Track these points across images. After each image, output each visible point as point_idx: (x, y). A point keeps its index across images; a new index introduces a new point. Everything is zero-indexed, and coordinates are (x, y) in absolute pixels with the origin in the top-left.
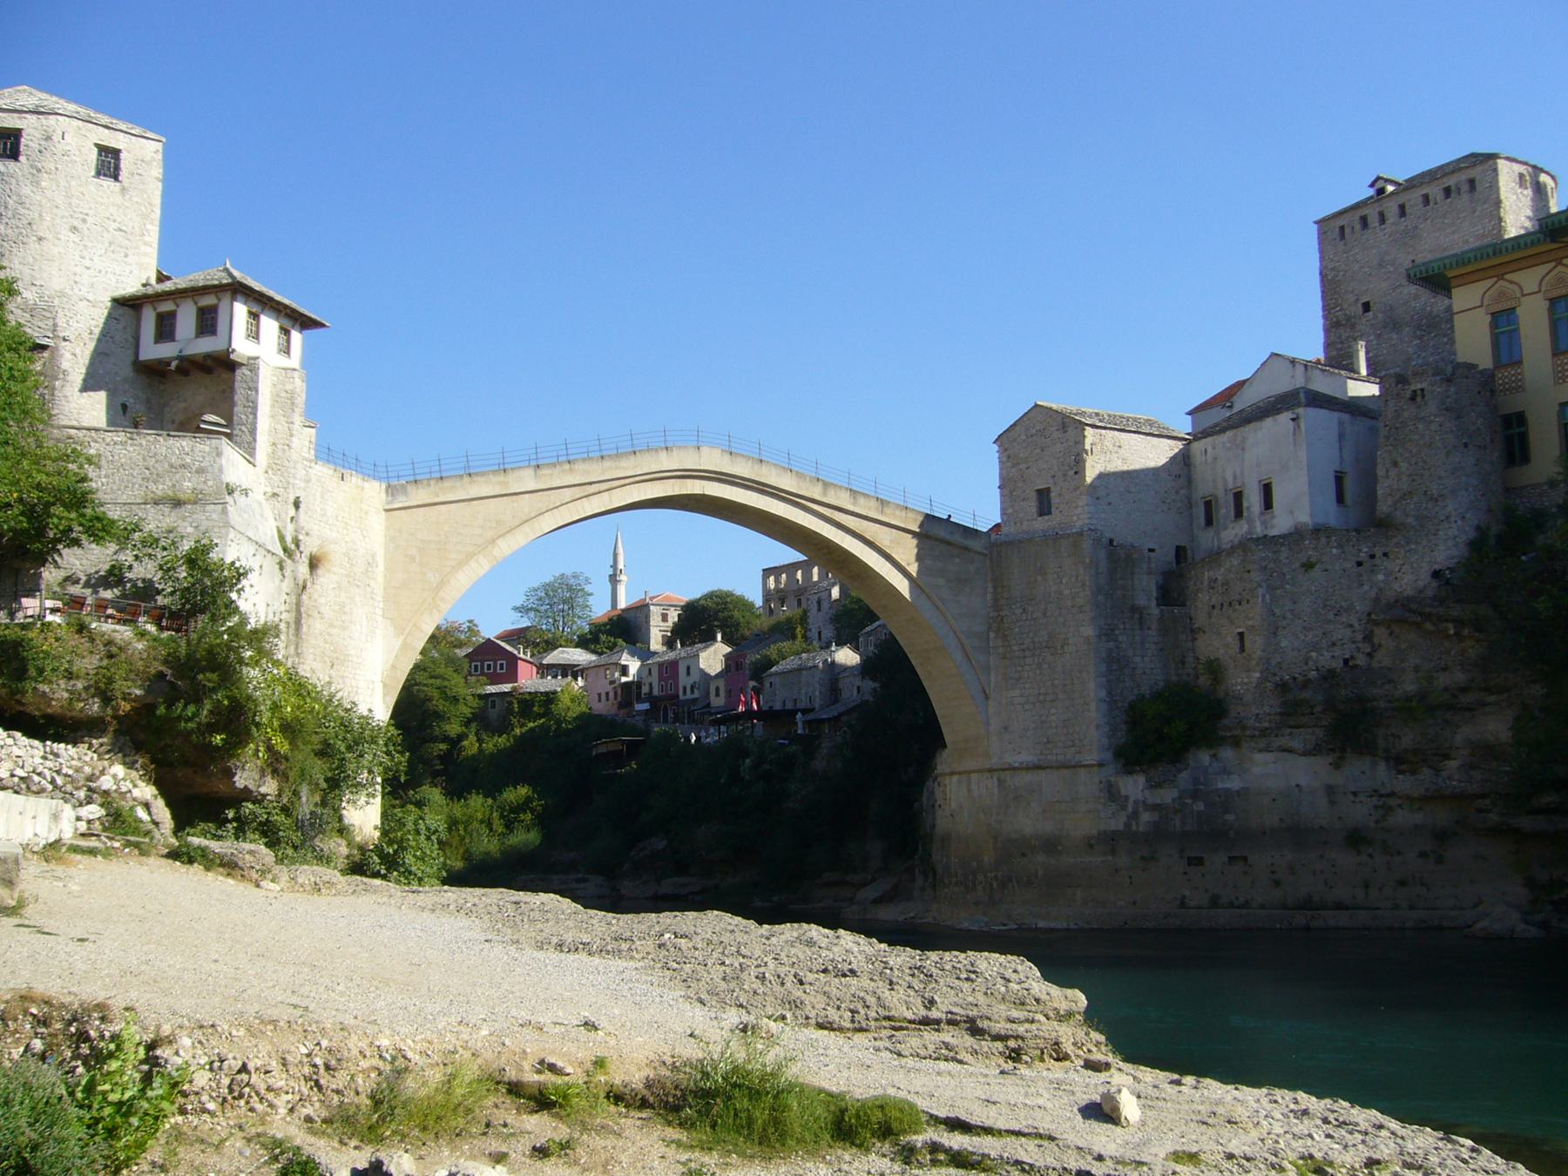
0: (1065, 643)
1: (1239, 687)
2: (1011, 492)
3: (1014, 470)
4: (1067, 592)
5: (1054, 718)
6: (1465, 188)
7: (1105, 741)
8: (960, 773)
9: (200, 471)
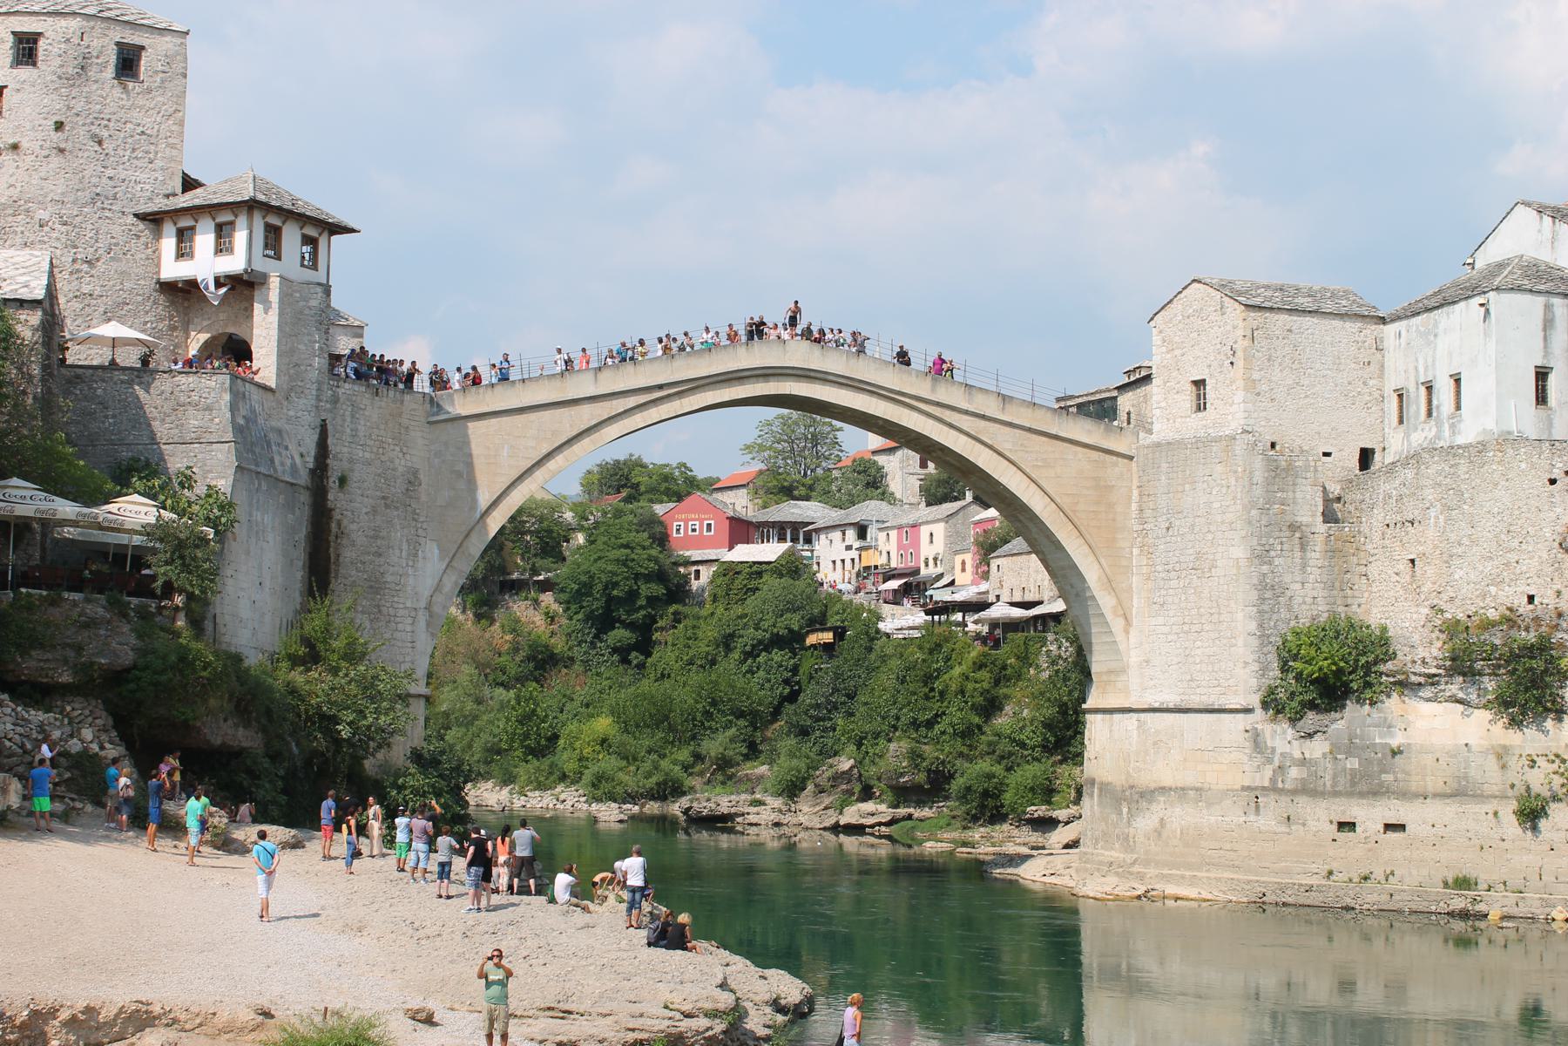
2: (1165, 383)
4: (1216, 505)
5: (1199, 652)
7: (1254, 682)
9: (209, 408)
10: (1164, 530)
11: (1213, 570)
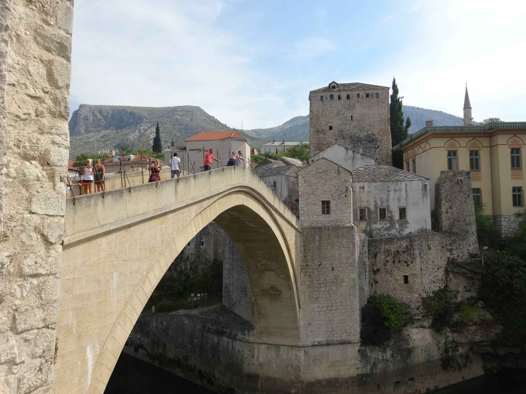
0: (342, 281)
1: (405, 300)
3: (308, 188)
4: (344, 255)
5: (336, 318)
6: (375, 96)
8: (268, 344)
10: (318, 266)
11: (343, 283)
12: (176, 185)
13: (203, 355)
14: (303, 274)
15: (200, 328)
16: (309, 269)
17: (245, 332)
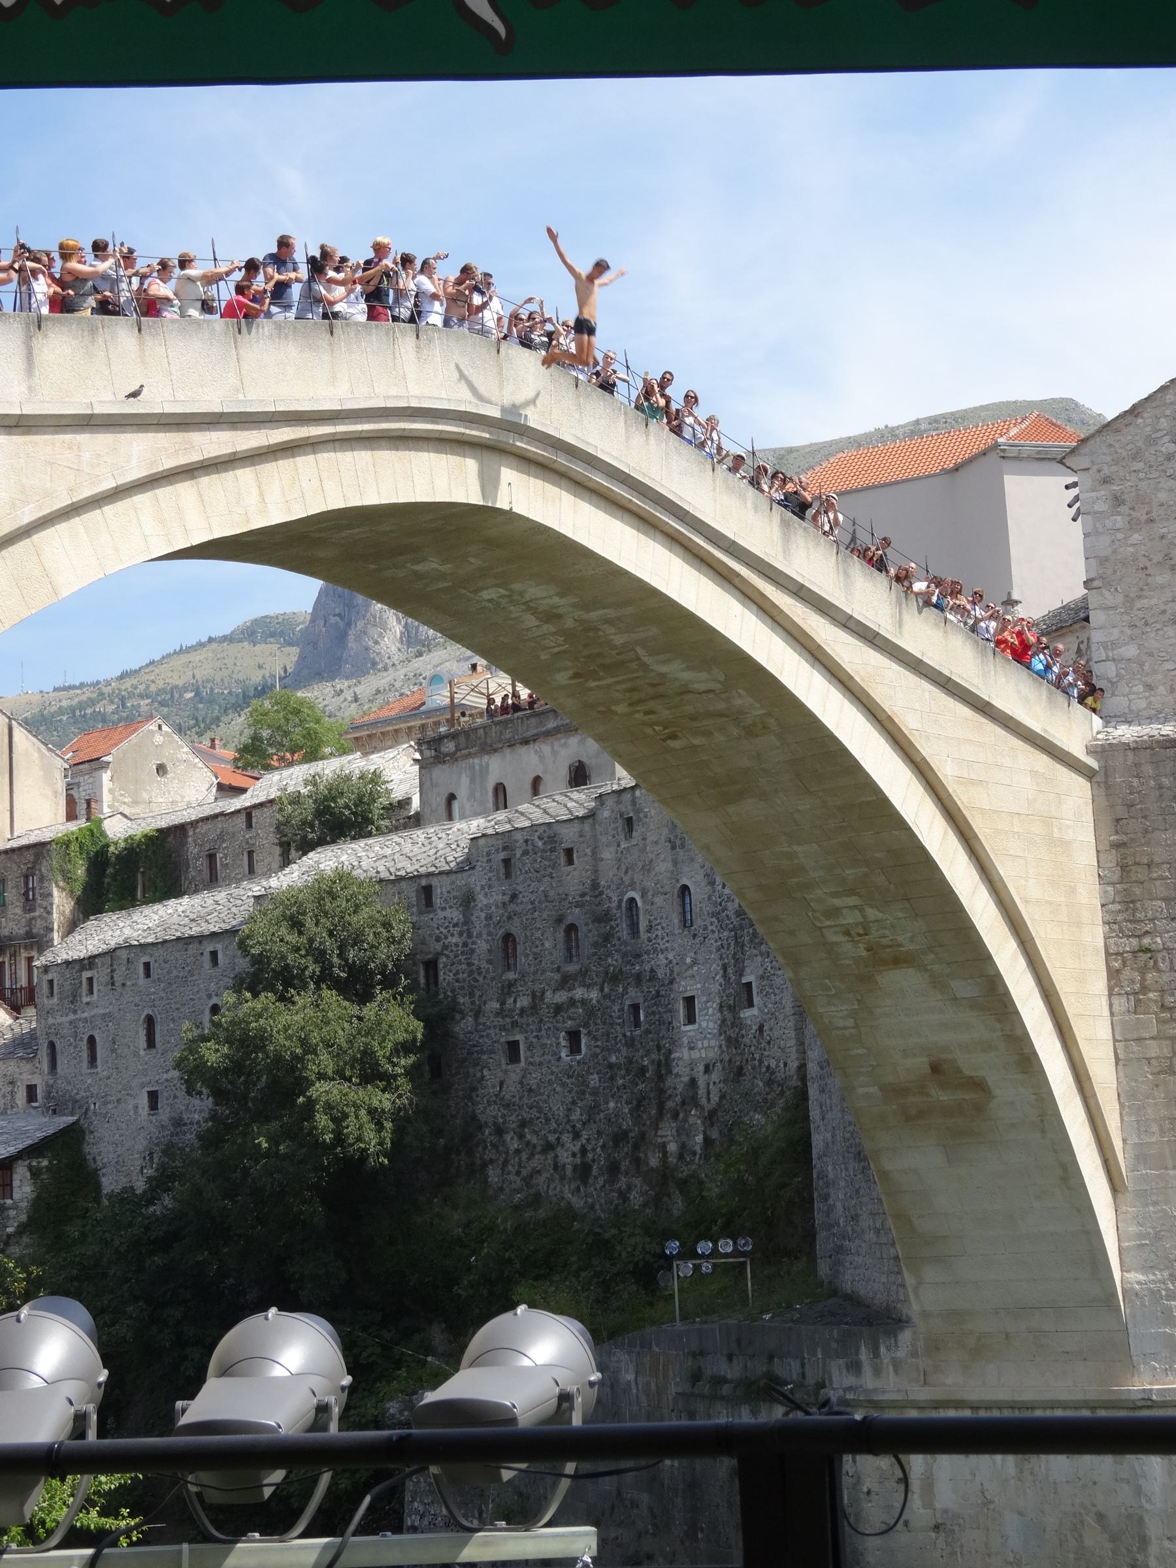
3: (1136, 537)
12: (29, 338)
13: (700, 1536)
14: (1124, 999)
15: (680, 1390)
16: (1159, 971)
17: (857, 1354)
